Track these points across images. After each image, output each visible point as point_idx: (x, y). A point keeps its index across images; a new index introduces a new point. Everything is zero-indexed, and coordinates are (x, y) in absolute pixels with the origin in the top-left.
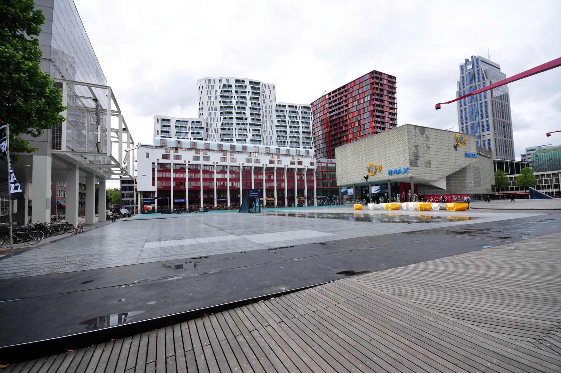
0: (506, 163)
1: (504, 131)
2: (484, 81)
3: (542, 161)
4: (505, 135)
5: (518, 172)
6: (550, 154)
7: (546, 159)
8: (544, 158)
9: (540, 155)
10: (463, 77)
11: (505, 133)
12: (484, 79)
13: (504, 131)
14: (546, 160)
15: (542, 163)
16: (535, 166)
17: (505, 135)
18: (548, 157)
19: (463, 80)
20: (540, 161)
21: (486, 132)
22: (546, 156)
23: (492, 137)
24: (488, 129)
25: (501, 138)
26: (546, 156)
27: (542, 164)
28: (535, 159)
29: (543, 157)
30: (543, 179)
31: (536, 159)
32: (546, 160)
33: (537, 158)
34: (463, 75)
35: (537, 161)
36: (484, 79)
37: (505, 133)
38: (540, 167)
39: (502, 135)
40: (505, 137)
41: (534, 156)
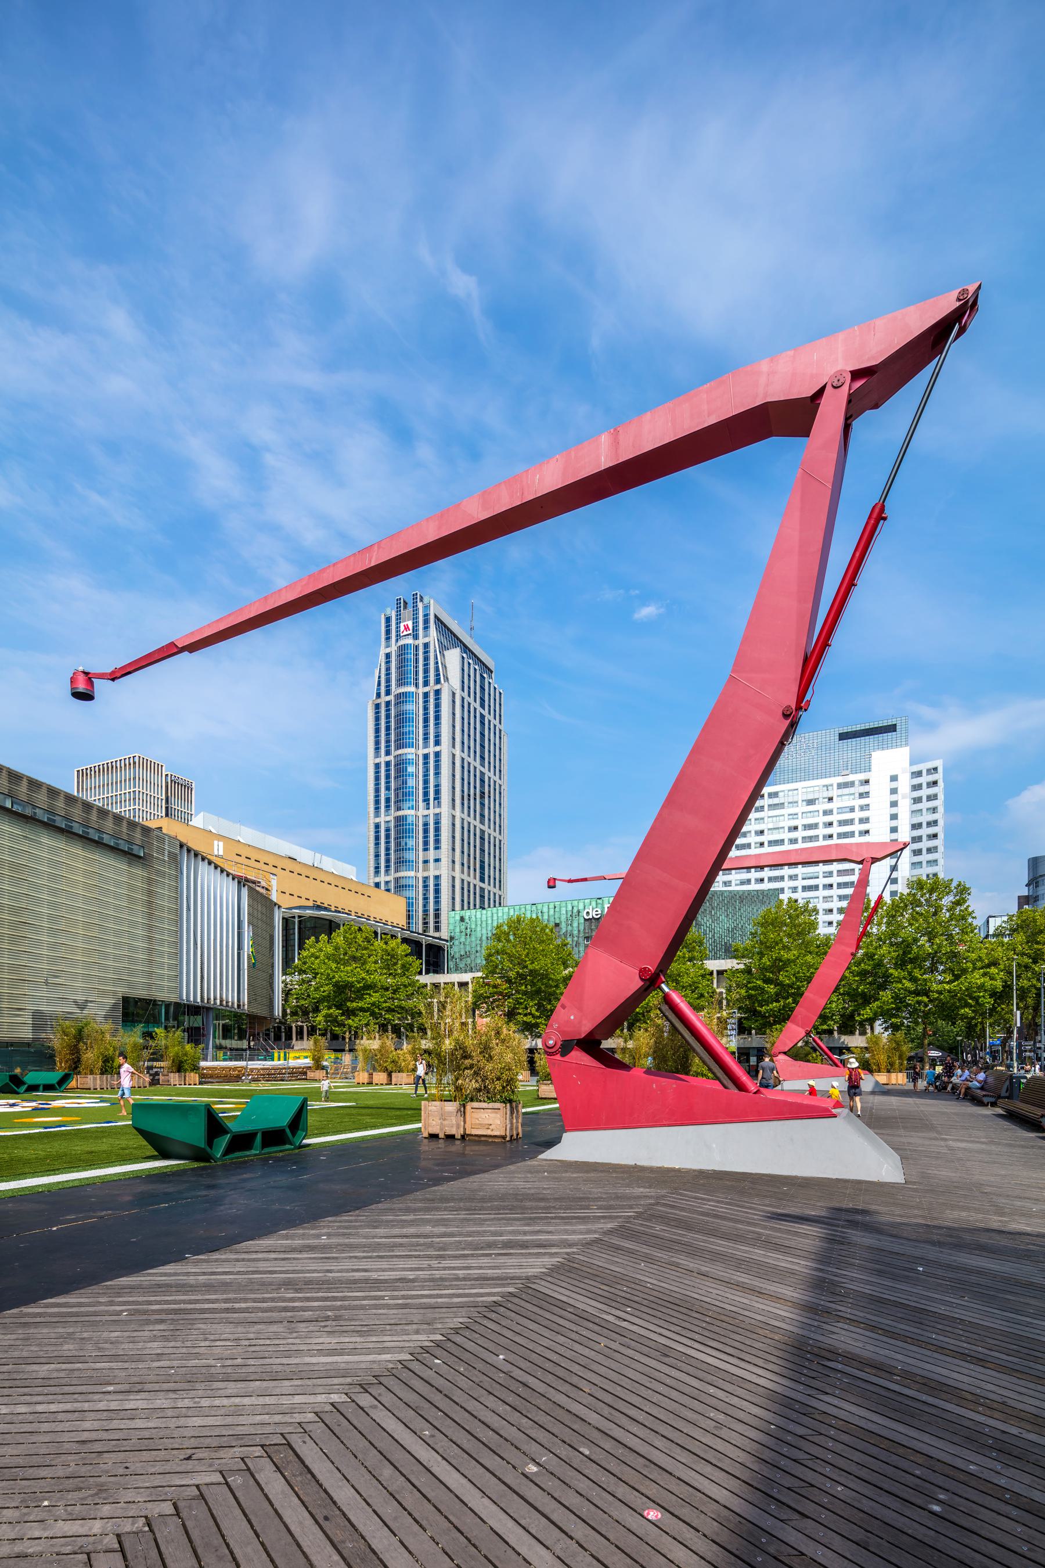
1: (482, 862)
2: (438, 687)
3: (473, 939)
4: (482, 873)
6: (495, 918)
7: (484, 931)
8: (479, 929)
11: (482, 868)
12: (438, 681)
13: (482, 862)
14: (484, 938)
15: (473, 945)
16: (457, 956)
17: (482, 873)
18: (489, 928)
20: (468, 940)
21: (432, 854)
22: (484, 925)
23: (444, 871)
24: (437, 841)
25: (471, 879)
26: (484, 925)
27: (474, 950)
28: (458, 930)
29: (476, 925)
30: (435, 1000)
31: (461, 932)
32: (484, 938)
33: (463, 927)
35: (463, 939)
36: (438, 681)
37: (482, 868)
38: (469, 961)
39: (475, 870)
40: (482, 880)
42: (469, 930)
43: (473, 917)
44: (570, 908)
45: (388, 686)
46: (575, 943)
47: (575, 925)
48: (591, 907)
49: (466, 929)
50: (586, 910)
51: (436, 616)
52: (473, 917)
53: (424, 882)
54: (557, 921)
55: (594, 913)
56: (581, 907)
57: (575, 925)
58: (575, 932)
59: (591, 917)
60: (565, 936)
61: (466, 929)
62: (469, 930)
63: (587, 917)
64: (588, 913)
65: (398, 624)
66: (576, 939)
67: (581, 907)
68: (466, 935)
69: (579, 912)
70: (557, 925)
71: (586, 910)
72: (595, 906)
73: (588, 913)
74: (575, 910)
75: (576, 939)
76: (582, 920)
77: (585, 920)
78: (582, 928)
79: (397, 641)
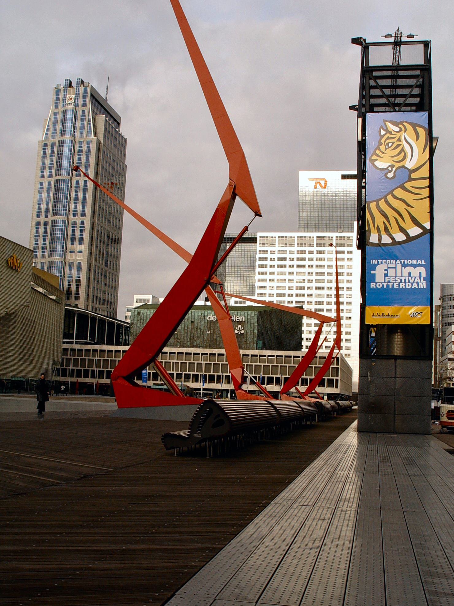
0: (94, 319)
5: (110, 343)
9: (143, 314)
10: (56, 114)
19: (55, 122)
28: (136, 319)
31: (137, 321)
33: (139, 318)
34: (56, 110)
35: (138, 325)
41: (136, 313)
42: (142, 320)
43: (145, 313)
44: (200, 314)
45: (54, 133)
46: (202, 332)
47: (202, 323)
48: (211, 315)
49: (141, 319)
50: (209, 316)
51: (92, 95)
52: (145, 313)
53: (70, 265)
54: (193, 320)
55: (213, 318)
56: (206, 314)
57: (202, 323)
58: (202, 327)
59: (211, 320)
60: (197, 329)
61: (141, 319)
62: (142, 320)
63: (209, 320)
64: (209, 318)
65: (65, 95)
66: (202, 330)
67: (206, 314)
68: (141, 322)
69: (205, 316)
70: (192, 322)
71: (209, 316)
72: (213, 315)
73: (209, 318)
74: (203, 315)
75: (202, 330)
76: (206, 321)
77: (208, 321)
78: (206, 325)
79: (63, 106)
